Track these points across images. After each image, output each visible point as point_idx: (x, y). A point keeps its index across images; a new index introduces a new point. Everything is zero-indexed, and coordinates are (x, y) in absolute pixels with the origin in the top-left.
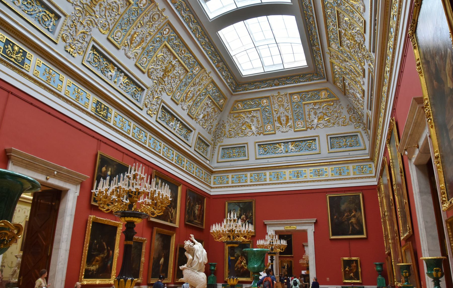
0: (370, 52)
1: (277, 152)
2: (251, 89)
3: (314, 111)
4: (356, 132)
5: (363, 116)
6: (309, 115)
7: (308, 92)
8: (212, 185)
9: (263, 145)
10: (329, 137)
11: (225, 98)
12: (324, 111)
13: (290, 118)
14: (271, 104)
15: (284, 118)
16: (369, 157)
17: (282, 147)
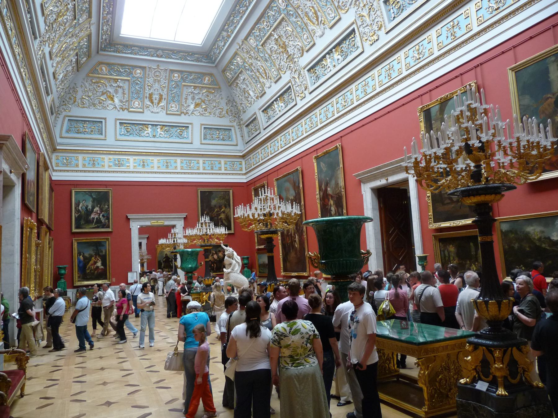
0: (304, 69)
1: (142, 134)
2: (125, 53)
3: (192, 95)
4: (230, 126)
5: (245, 112)
6: (186, 99)
7: (191, 73)
8: (55, 168)
9: (125, 123)
10: (203, 127)
11: (89, 56)
12: (203, 98)
13: (164, 97)
14: (144, 77)
15: (158, 97)
16: (241, 154)
17: (150, 130)
